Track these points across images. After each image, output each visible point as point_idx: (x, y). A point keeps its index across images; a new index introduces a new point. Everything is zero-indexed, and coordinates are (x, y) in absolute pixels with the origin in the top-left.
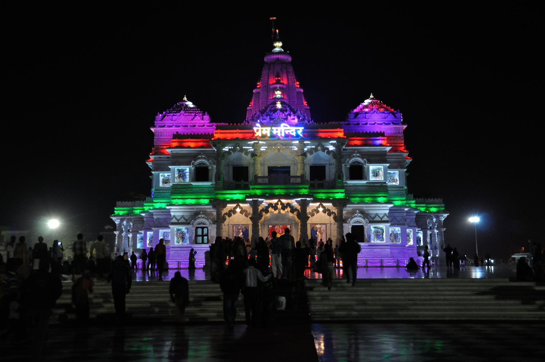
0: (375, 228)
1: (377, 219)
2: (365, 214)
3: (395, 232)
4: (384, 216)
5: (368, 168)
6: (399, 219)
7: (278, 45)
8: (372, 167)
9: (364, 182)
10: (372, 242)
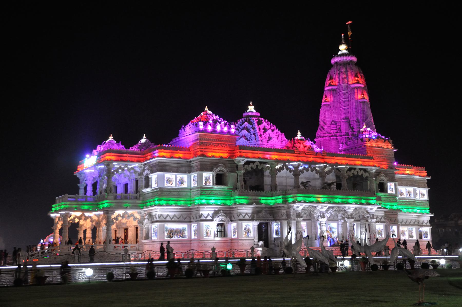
1: (155, 220)
2: (150, 215)
4: (167, 217)
5: (151, 178)
6: (198, 216)
7: (343, 48)
8: (154, 177)
9: (148, 190)
10: (153, 238)
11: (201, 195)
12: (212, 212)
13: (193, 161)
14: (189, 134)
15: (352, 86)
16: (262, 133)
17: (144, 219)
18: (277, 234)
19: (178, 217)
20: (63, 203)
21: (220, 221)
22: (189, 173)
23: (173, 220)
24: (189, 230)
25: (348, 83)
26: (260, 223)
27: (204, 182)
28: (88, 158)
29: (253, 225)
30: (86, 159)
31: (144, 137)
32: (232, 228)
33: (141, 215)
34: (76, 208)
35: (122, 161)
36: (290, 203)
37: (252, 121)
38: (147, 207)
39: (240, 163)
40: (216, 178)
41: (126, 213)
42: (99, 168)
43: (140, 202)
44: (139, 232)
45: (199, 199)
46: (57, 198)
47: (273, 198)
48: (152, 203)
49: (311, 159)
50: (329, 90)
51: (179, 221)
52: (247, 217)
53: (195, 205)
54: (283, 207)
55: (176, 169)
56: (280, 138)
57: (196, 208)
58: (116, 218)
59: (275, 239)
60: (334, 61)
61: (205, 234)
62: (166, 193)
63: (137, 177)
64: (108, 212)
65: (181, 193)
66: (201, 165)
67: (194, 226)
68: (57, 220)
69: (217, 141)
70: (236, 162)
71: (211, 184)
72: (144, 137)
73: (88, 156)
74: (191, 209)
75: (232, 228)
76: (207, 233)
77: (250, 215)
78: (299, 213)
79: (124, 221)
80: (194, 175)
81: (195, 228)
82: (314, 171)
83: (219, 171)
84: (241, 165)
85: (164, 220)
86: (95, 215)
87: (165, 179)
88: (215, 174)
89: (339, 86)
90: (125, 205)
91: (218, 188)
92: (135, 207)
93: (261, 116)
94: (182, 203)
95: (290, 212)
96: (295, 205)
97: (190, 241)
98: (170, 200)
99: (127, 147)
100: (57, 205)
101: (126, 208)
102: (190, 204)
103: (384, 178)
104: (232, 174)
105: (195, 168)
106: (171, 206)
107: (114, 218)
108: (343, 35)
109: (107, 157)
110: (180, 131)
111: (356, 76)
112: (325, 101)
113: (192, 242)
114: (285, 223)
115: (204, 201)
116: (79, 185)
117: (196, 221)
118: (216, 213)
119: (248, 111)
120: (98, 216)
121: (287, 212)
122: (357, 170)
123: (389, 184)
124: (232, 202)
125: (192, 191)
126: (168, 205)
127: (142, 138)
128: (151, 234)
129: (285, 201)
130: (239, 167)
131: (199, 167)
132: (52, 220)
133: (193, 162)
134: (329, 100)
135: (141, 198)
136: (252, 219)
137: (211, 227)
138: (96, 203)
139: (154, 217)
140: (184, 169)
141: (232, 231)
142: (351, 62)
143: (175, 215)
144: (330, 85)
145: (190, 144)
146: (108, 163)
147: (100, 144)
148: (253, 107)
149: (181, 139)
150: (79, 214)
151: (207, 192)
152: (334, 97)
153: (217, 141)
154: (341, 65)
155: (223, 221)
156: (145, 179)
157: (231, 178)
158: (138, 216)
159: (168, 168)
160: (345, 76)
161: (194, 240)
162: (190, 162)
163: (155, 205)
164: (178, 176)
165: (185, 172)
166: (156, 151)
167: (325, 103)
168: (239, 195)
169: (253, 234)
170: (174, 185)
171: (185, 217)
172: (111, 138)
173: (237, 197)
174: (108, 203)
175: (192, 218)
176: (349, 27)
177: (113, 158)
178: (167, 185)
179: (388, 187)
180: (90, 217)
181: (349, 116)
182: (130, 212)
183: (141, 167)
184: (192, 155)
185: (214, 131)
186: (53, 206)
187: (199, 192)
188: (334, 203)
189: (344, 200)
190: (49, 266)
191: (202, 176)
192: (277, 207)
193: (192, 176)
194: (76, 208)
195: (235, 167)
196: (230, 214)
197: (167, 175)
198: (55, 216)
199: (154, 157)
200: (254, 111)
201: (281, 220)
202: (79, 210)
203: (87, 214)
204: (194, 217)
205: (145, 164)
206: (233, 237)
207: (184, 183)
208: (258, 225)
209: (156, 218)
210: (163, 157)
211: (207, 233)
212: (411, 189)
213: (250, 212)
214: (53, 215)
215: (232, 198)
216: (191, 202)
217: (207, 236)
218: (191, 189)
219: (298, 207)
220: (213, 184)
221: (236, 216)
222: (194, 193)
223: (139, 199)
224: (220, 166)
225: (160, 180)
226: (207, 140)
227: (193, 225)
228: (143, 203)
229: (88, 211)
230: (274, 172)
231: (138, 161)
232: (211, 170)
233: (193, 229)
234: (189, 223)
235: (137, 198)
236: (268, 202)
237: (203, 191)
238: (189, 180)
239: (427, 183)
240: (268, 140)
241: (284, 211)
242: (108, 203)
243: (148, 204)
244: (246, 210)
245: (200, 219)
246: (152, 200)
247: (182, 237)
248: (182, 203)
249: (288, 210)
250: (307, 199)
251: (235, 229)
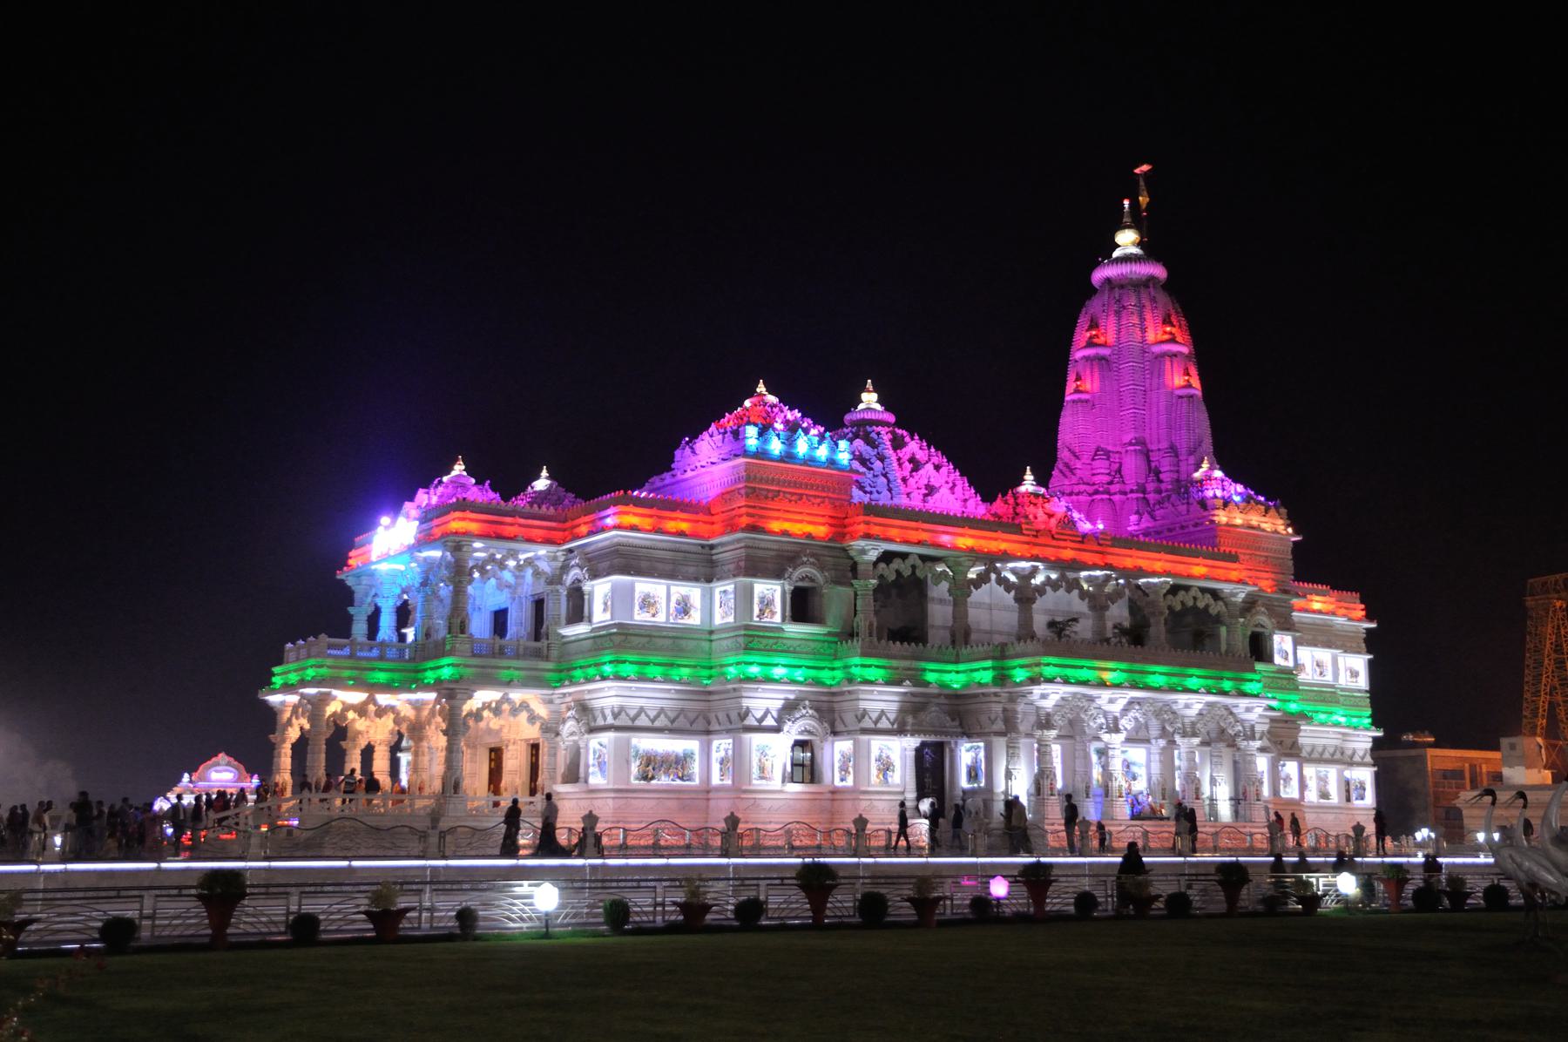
1: (600, 722)
2: (584, 709)
5: (591, 594)
6: (734, 716)
7: (1127, 240)
8: (600, 590)
9: (581, 629)
11: (747, 649)
12: (779, 704)
13: (722, 544)
14: (707, 463)
15: (1157, 349)
16: (906, 473)
17: (564, 721)
18: (973, 774)
19: (672, 715)
20: (311, 662)
21: (801, 733)
22: (709, 581)
23: (657, 724)
24: (707, 760)
25: (1144, 341)
26: (923, 744)
27: (756, 611)
28: (387, 528)
29: (900, 750)
30: (380, 530)
31: (544, 473)
32: (837, 757)
33: (552, 707)
34: (350, 678)
35: (499, 537)
36: (1021, 684)
37: (874, 435)
38: (572, 683)
39: (866, 558)
40: (792, 599)
41: (505, 699)
42: (425, 559)
43: (550, 666)
44: (544, 759)
45: (738, 663)
46: (289, 645)
47: (962, 667)
48: (591, 671)
49: (1068, 554)
50: (1086, 358)
51: (674, 729)
52: (884, 724)
53: (728, 682)
54: (996, 694)
55: (668, 567)
56: (958, 489)
57: (727, 691)
58: (477, 716)
59: (964, 792)
60: (1099, 275)
61: (755, 771)
62: (636, 640)
63: (541, 588)
64: (451, 692)
65: (683, 643)
66: (748, 558)
67: (722, 746)
68: (287, 715)
69: (795, 485)
70: (852, 553)
71: (778, 618)
72: (544, 473)
73: (385, 520)
74: (710, 693)
75: (837, 757)
76: (762, 769)
77: (892, 716)
78: (1048, 714)
79: (495, 723)
80: (724, 589)
81: (722, 754)
82: (1076, 592)
83: (802, 579)
84: (867, 563)
85: (629, 723)
86: (410, 702)
87: (637, 596)
88: (789, 588)
89: (1119, 348)
90: (505, 674)
91: (796, 630)
92: (534, 681)
93: (898, 424)
94: (685, 673)
95: (1015, 712)
96: (1037, 690)
97: (707, 791)
98: (647, 664)
99: (506, 499)
100: (292, 666)
101: (509, 684)
102: (710, 677)
103: (1263, 619)
104: (841, 589)
105: (725, 568)
106: (652, 680)
107: (470, 714)
108: (1126, 203)
109: (455, 526)
110: (678, 453)
111: (1167, 321)
112: (1077, 391)
113: (711, 795)
114: (1000, 743)
115: (754, 670)
116: (351, 610)
117: (728, 731)
118: (789, 708)
119: (861, 407)
120: (418, 706)
121: (1005, 710)
122: (1193, 592)
123: (1277, 638)
124: (839, 674)
125: (714, 637)
126: (642, 678)
127: (538, 477)
128: (587, 766)
129: (1002, 679)
130: (860, 568)
131: (742, 564)
132: (271, 714)
133: (720, 549)
134: (1088, 386)
135: (554, 653)
136: (900, 730)
137: (774, 751)
138: (411, 666)
139: (598, 713)
140: (692, 570)
141: (837, 765)
142: (1149, 281)
143: (662, 711)
144: (1091, 344)
145: (713, 493)
146: (457, 543)
147: (426, 486)
148: (874, 396)
149: (679, 477)
150: (357, 697)
151: (765, 641)
152: (1102, 378)
153: (795, 485)
154: (1122, 287)
155: (810, 733)
156: (569, 596)
157: (836, 600)
158: (542, 711)
159: (644, 564)
160: (1135, 320)
161: (719, 789)
162: (712, 547)
163: (604, 678)
164: (673, 589)
165: (696, 579)
166: (609, 511)
167: (1076, 397)
168: (864, 655)
169: (902, 777)
170: (661, 619)
171: (692, 716)
172: (459, 469)
173: (857, 660)
174: (453, 665)
175: (714, 721)
176: (1142, 183)
177: (474, 527)
178: (640, 617)
179: (1276, 647)
180: (392, 709)
181: (1147, 436)
182: (517, 695)
183: (555, 559)
184: (716, 527)
185: (789, 457)
186: (276, 670)
187: (741, 640)
188: (1147, 688)
189: (1174, 680)
190: (345, 863)
191: (749, 592)
192: (976, 696)
193: (717, 591)
194: (350, 678)
195: (851, 570)
196: (831, 712)
197: (644, 586)
198: (283, 703)
199: (604, 529)
200: (878, 407)
201: (988, 734)
202: (361, 684)
203: (383, 699)
204: (722, 716)
205: (571, 551)
206: (838, 783)
207: (692, 612)
208: (919, 752)
209: (605, 718)
210: (633, 528)
211: (762, 769)
212: (1324, 655)
213: (894, 707)
214: (274, 699)
215: (837, 664)
216: (713, 672)
217: (761, 778)
218: (711, 632)
219: (1044, 696)
220: (784, 619)
221: (849, 718)
222: (724, 643)
223: (547, 659)
224: (804, 563)
225: (621, 598)
226: (767, 482)
227: (715, 743)
228: (560, 671)
229: (387, 688)
230: (961, 590)
231: (548, 541)
232: (777, 575)
233: (716, 756)
234: (705, 738)
235: (538, 655)
236: (947, 678)
237: (752, 638)
238: (708, 605)
239: (1366, 641)
240: (925, 495)
241: (998, 708)
242: (453, 665)
243: (578, 673)
244: (883, 701)
245: (740, 724)
246: (592, 661)
247: (681, 779)
248: (685, 673)
249: (1009, 706)
250: (1069, 672)
251: (845, 760)
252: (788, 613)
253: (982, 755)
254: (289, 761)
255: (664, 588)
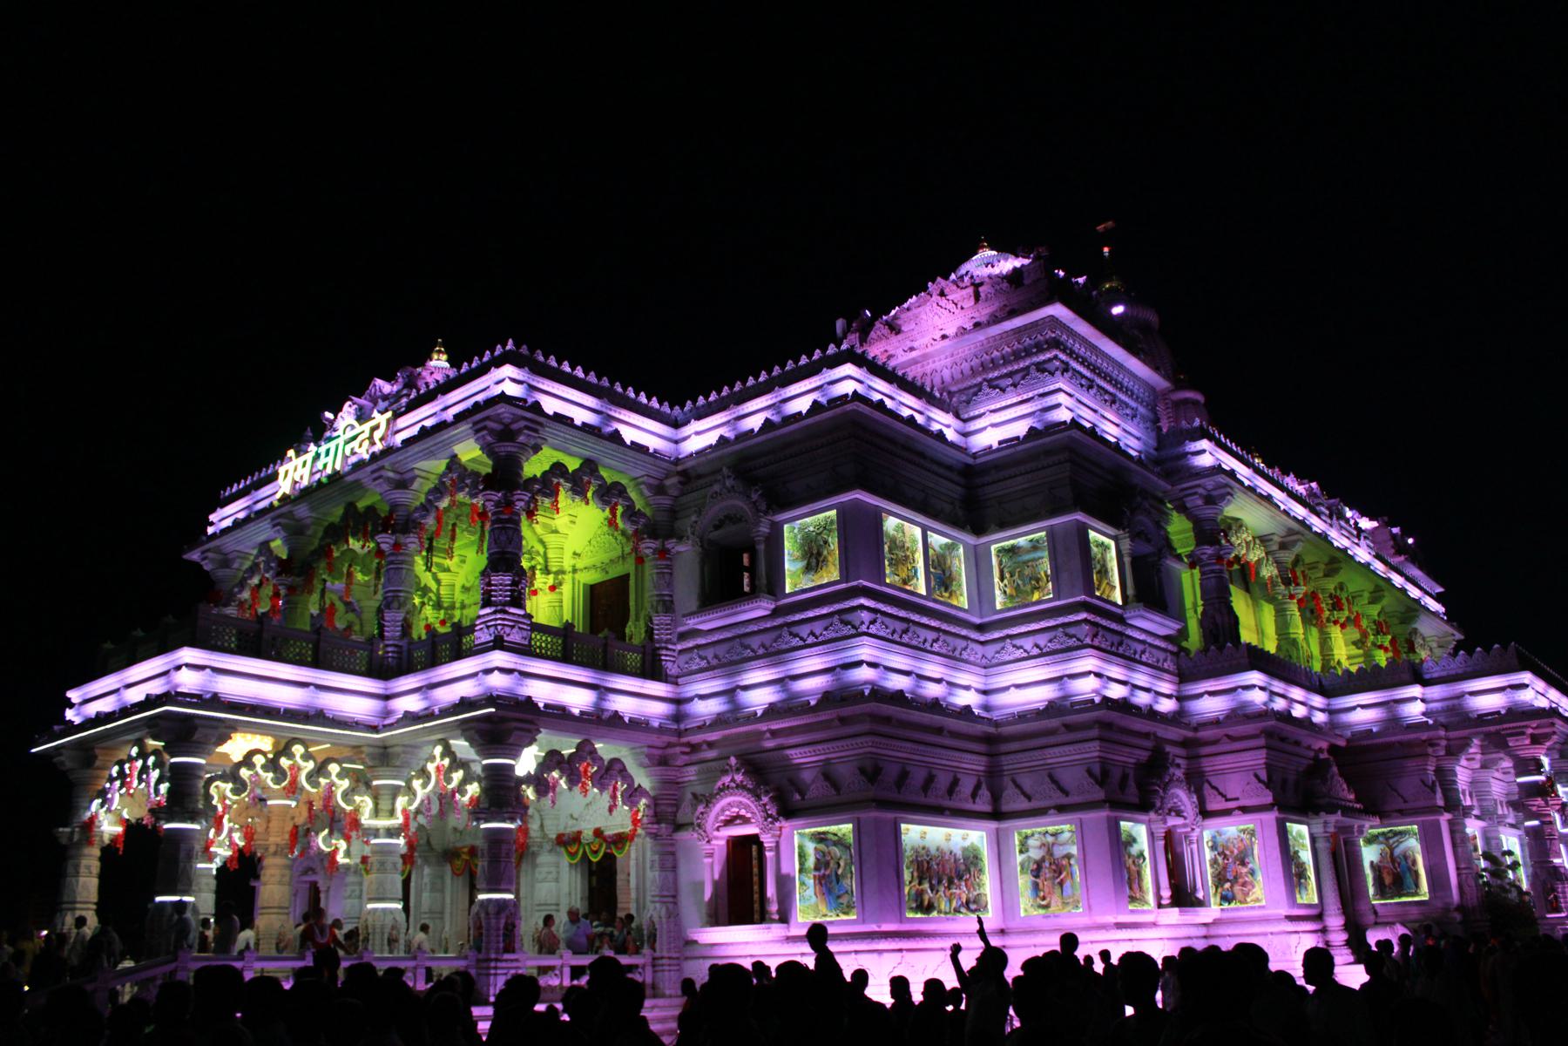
0: (820, 838)
3: (1059, 852)
54: (1431, 743)
71: (1117, 597)
81: (1035, 854)
117: (1062, 809)
128: (785, 883)
175: (1010, 791)
186: (74, 695)
192: (1369, 748)
193: (994, 548)
204: (1027, 782)
232: (1112, 517)
234: (993, 825)
252: (1130, 592)
253: (1413, 845)
254: (95, 882)
255: (917, 531)
